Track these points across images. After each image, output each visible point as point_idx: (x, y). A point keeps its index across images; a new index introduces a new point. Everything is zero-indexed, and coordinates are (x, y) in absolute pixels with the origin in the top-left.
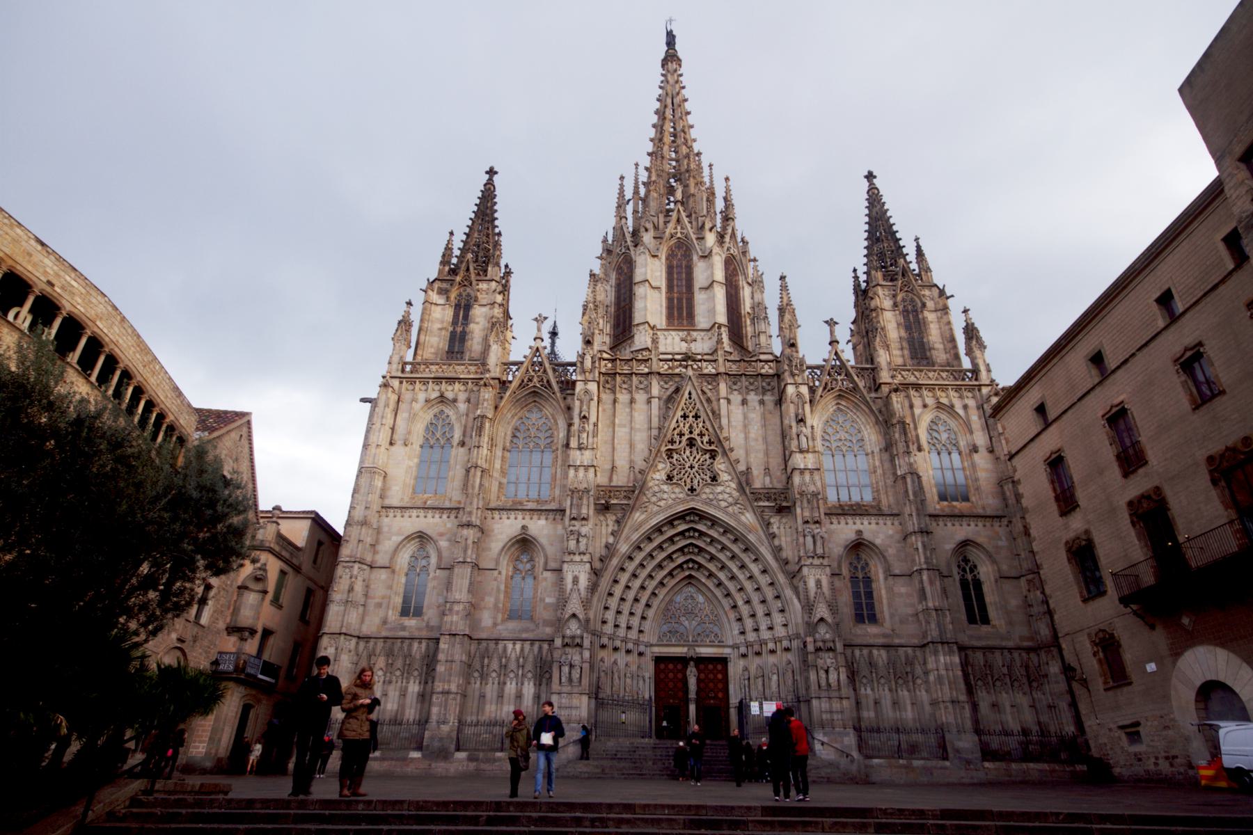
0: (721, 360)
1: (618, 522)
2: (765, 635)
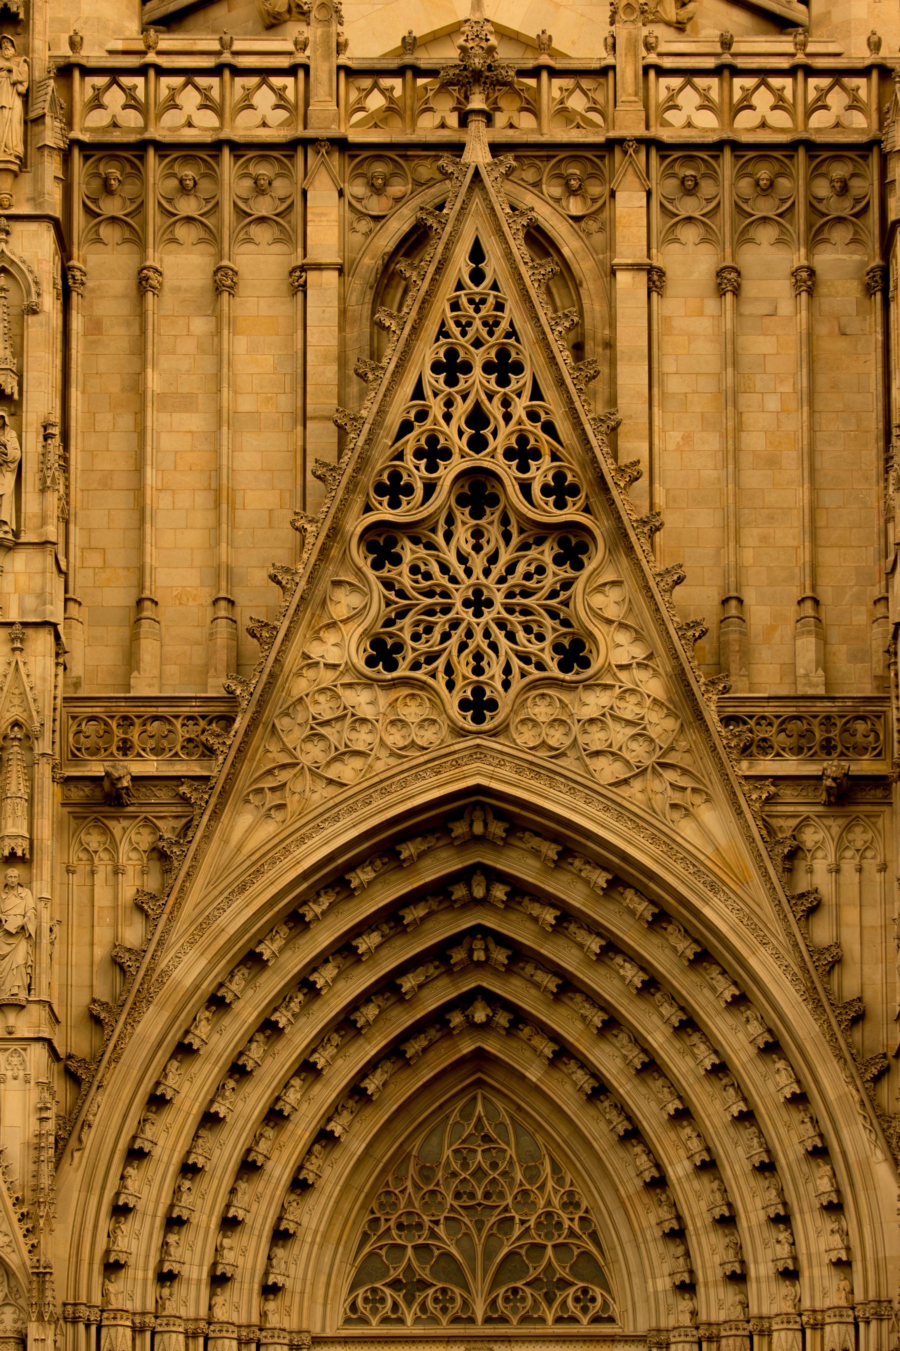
0: (628, 72)
1: (161, 855)
2: (768, 1297)
